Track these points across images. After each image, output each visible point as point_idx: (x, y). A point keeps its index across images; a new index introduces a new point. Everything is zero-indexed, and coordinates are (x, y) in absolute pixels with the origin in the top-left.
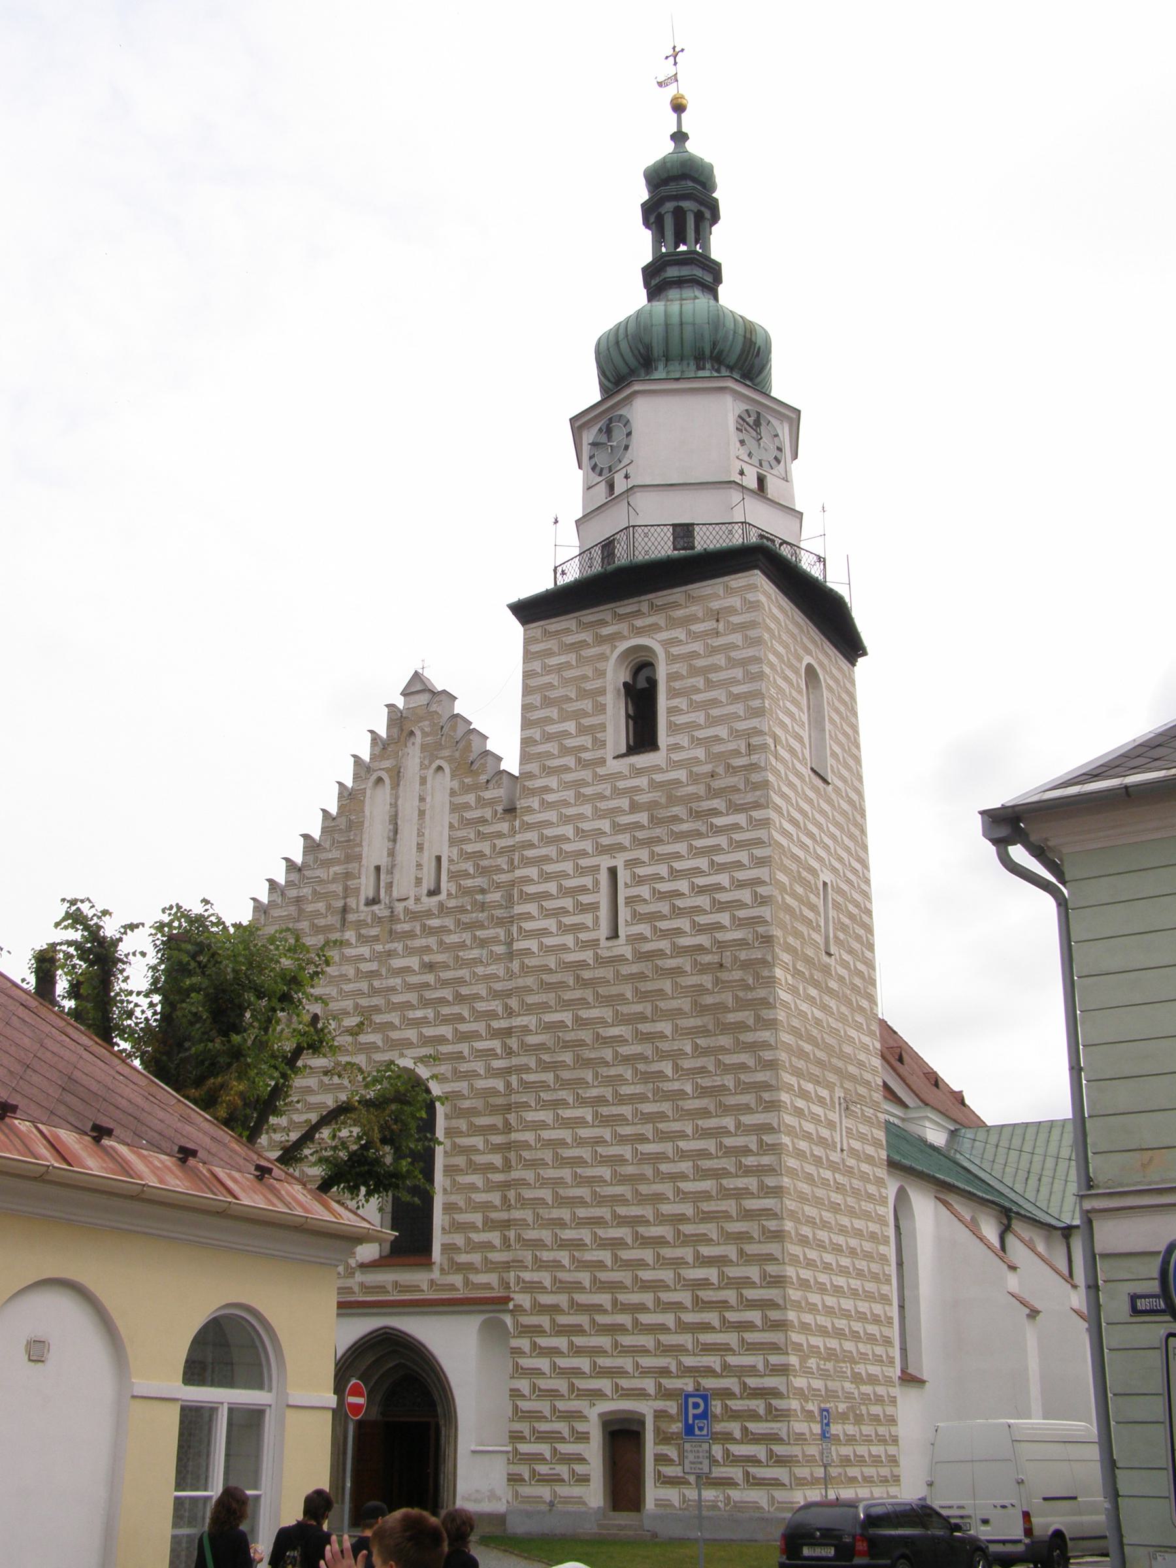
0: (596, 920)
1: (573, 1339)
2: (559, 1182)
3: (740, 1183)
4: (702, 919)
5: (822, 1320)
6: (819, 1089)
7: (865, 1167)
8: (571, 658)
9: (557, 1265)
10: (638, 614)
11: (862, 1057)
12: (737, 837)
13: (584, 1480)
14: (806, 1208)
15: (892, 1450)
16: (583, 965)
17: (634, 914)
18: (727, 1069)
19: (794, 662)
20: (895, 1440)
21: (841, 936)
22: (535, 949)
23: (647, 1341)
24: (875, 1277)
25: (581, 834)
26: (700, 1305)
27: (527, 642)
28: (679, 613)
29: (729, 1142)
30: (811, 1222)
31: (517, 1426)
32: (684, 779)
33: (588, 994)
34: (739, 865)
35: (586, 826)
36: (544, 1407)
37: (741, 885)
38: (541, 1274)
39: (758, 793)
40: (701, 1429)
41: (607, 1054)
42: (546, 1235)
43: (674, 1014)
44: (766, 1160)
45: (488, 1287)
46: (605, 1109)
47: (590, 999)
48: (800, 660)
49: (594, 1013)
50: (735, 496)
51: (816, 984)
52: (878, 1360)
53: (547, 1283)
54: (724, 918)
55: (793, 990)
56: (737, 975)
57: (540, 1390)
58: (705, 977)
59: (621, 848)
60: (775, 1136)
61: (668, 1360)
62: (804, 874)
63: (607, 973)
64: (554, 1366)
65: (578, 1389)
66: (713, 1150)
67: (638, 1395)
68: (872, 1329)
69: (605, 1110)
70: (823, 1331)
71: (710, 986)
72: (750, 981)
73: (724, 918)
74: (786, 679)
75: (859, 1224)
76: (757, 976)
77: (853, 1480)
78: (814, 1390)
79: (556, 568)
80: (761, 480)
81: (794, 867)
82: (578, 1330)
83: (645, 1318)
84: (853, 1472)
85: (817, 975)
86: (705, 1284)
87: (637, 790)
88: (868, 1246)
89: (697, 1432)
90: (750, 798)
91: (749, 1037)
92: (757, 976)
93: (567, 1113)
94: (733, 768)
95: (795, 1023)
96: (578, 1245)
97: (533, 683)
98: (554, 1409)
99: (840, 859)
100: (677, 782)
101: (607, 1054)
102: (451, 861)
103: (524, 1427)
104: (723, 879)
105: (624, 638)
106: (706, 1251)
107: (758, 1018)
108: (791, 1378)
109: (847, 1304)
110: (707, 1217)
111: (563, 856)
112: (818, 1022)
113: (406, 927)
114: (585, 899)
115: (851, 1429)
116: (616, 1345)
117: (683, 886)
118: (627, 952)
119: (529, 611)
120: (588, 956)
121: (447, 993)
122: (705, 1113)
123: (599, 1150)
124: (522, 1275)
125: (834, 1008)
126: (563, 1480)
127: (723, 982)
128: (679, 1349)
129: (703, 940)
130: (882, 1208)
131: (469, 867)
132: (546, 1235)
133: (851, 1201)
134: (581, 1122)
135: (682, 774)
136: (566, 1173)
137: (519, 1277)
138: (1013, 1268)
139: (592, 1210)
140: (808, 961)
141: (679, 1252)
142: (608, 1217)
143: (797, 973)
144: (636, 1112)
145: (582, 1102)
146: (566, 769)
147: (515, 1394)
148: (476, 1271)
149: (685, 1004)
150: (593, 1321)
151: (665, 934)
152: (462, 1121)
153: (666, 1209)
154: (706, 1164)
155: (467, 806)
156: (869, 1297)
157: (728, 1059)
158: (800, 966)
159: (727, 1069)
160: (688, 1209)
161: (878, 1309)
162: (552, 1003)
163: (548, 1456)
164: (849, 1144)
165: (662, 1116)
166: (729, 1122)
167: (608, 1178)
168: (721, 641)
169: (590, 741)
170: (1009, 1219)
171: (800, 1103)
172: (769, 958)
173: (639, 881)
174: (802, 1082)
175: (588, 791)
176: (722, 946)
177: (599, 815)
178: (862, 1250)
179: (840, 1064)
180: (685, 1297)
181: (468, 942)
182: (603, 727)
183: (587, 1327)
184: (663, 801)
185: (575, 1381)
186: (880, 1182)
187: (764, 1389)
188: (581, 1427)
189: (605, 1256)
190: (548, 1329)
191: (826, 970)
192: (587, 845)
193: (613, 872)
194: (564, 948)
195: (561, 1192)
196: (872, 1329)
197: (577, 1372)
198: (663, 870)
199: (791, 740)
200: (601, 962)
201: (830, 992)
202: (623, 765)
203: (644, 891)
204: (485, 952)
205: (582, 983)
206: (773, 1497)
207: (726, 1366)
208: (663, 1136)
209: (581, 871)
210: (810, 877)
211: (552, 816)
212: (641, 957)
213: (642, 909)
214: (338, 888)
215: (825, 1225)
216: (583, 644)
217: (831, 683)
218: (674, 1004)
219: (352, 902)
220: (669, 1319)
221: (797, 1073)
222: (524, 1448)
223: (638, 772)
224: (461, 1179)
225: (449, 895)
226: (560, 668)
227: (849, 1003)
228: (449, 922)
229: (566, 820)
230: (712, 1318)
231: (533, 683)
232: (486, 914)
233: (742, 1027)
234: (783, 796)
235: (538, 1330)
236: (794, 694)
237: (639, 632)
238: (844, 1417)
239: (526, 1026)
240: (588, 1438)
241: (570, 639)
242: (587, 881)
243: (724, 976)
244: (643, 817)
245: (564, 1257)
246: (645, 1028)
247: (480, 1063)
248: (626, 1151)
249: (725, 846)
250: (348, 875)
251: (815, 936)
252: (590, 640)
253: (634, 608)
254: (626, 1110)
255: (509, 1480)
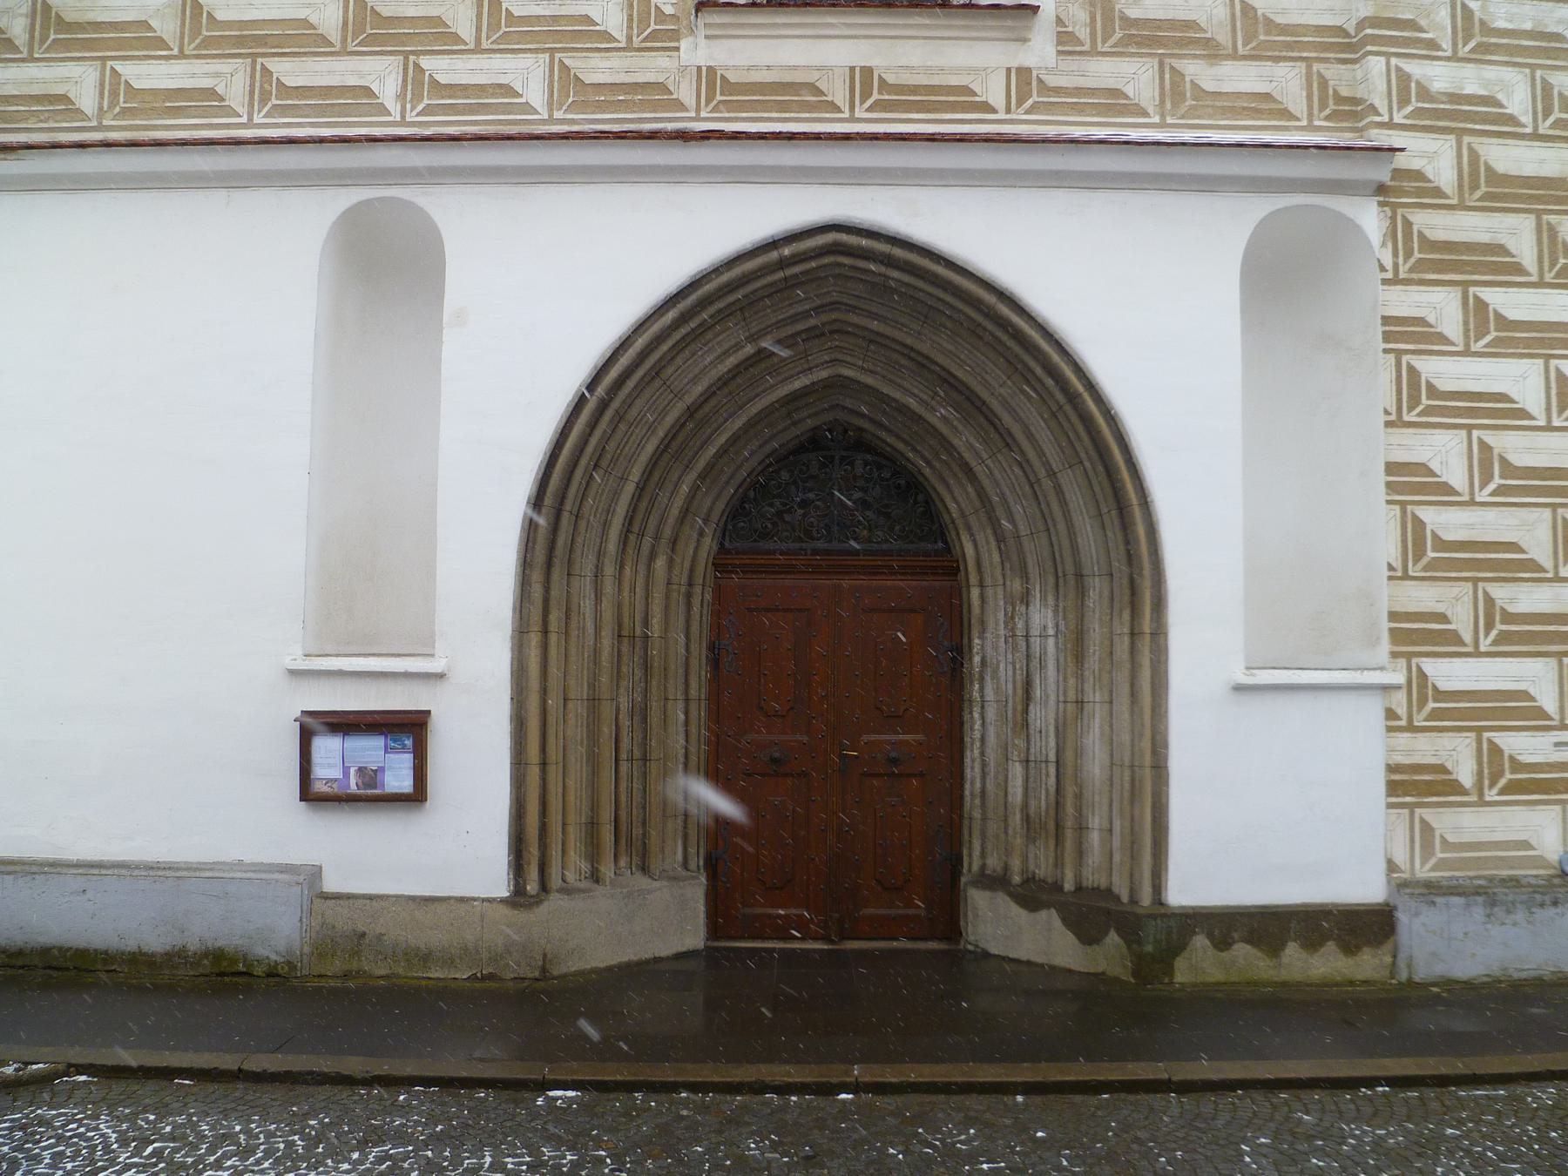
31: (1422, 597)
38: (1491, 72)
45: (1264, 105)
57: (1508, 469)
103: (1453, 601)
124: (1415, 69)
137: (1404, 78)
147: (1410, 483)
148: (1212, 52)
222: (1449, 673)
255: (1393, 788)
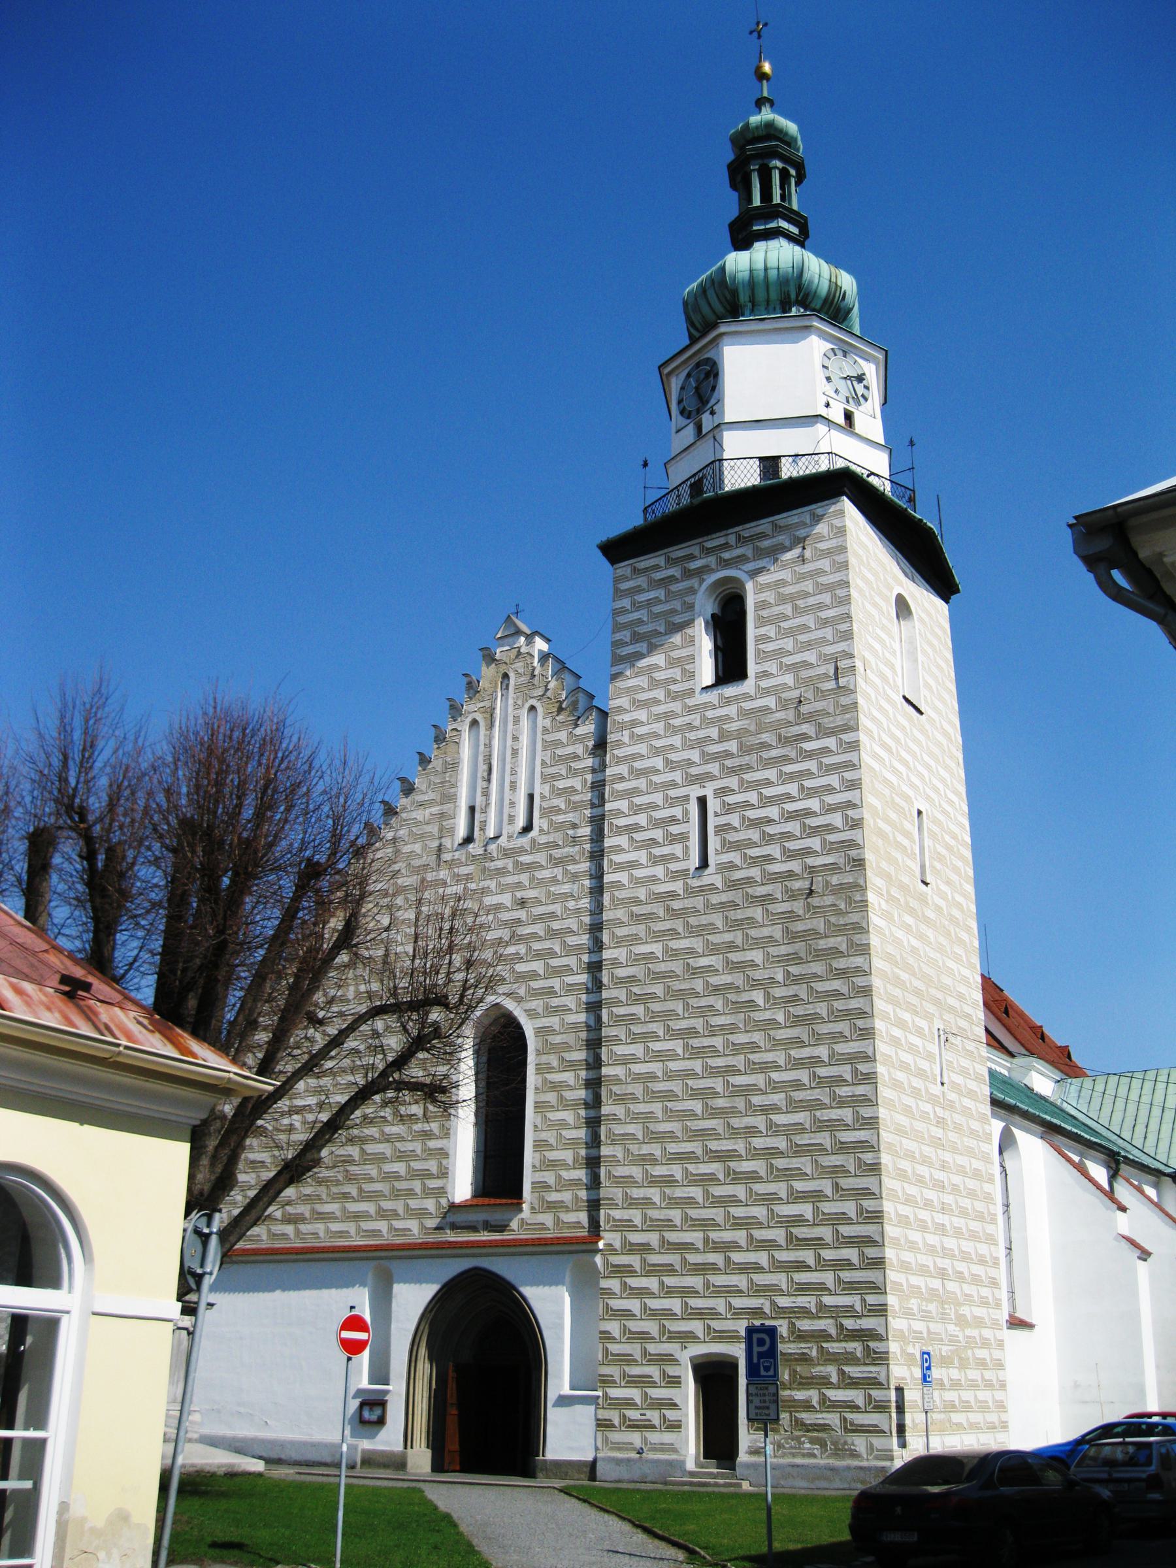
0: (686, 850)
1: (664, 1279)
2: (649, 1116)
3: (834, 1114)
4: (792, 845)
5: (923, 1259)
6: (917, 1019)
7: (967, 1102)
8: (660, 593)
9: (647, 1202)
10: (726, 546)
11: (962, 989)
12: (826, 761)
13: (676, 1426)
14: (905, 1141)
15: (999, 1395)
16: (673, 895)
17: (724, 842)
18: (819, 996)
19: (885, 591)
20: (1003, 1386)
21: (938, 865)
22: (625, 881)
23: (740, 1281)
24: (980, 1217)
25: (671, 765)
26: (795, 1242)
27: (617, 580)
28: (766, 543)
29: (822, 1071)
30: (910, 1156)
32: (773, 706)
33: (678, 925)
34: (829, 789)
35: (674, 757)
36: (635, 1349)
37: (831, 809)
39: (848, 716)
40: (767, 1369)
41: (698, 985)
42: (636, 1172)
43: (763, 943)
44: (860, 1090)
46: (696, 1041)
47: (680, 930)
48: (891, 589)
49: (684, 944)
50: (821, 428)
51: (912, 911)
52: (985, 1303)
53: (637, 1221)
54: (815, 843)
55: (887, 916)
56: (829, 900)
57: (630, 1332)
58: (795, 903)
59: (710, 777)
60: (870, 1065)
61: (761, 1300)
62: (897, 800)
63: (698, 902)
64: (645, 1307)
65: (670, 1332)
66: (806, 1080)
67: (731, 1337)
68: (977, 1269)
69: (695, 1043)
70: (924, 1271)
71: (801, 912)
72: (842, 906)
73: (815, 843)
74: (875, 605)
75: (961, 1160)
76: (849, 900)
77: (959, 1426)
78: (915, 1332)
79: (645, 510)
80: (849, 416)
81: (887, 792)
82: (669, 1270)
83: (737, 1257)
84: (957, 1418)
85: (913, 903)
86: (799, 1220)
87: (727, 719)
88: (971, 1184)
89: (763, 1373)
90: (839, 721)
91: (841, 963)
92: (849, 900)
93: (657, 1046)
94: (822, 691)
95: (890, 949)
96: (669, 1181)
97: (622, 619)
98: (645, 1352)
99: (936, 790)
100: (766, 710)
101: (698, 985)
102: (543, 797)
104: (814, 804)
105: (713, 571)
106: (799, 1186)
107: (851, 944)
108: (890, 1318)
109: (950, 1243)
110: (799, 1151)
111: (654, 788)
112: (914, 950)
113: (499, 864)
114: (675, 829)
115: (955, 1373)
116: (707, 1285)
117: (773, 812)
118: (718, 881)
119: (618, 550)
120: (678, 886)
121: (539, 929)
122: (798, 1043)
123: (690, 1082)
125: (931, 937)
126: (654, 1427)
127: (815, 907)
128: (775, 1289)
129: (795, 866)
130: (986, 1145)
131: (560, 803)
132: (636, 1172)
133: (952, 1136)
134: (671, 1055)
135: (771, 702)
136: (657, 1108)
137: (609, 1215)
138: (1123, 1209)
139: (684, 1145)
140: (903, 887)
141: (771, 1188)
142: (699, 1152)
143: (891, 899)
144: (727, 1043)
145: (672, 1034)
146: (656, 702)
148: (568, 1210)
149: (777, 932)
150: (684, 1261)
151: (754, 861)
152: (552, 1057)
153: (758, 1142)
154: (799, 1095)
155: (558, 743)
156: (974, 1236)
157: (821, 987)
158: (895, 892)
159: (819, 996)
160: (781, 1143)
161: (983, 1249)
162: (642, 935)
163: (638, 1401)
164: (949, 1077)
165: (754, 1047)
166: (822, 1052)
167: (699, 1112)
168: (808, 567)
169: (679, 673)
170: (1117, 1163)
171: (897, 1032)
172: (861, 882)
173: (729, 809)
174: (898, 1010)
175: (677, 722)
176: (812, 871)
177: (689, 745)
178: (966, 1188)
179: (939, 995)
180: (779, 1235)
181: (560, 877)
182: (692, 659)
183: (678, 1267)
184: (752, 728)
185: (666, 1323)
186: (982, 1119)
187: (862, 1330)
188: (671, 1371)
189: (696, 1192)
190: (638, 1270)
191: (923, 899)
192: (677, 776)
193: (702, 801)
194: (654, 879)
195: (652, 1127)
196: (977, 1269)
197: (668, 1314)
198: (752, 797)
199: (882, 666)
200: (691, 892)
201: (927, 921)
202: (713, 696)
203: (734, 820)
204: (576, 886)
205: (674, 914)
206: (872, 1445)
207: (821, 1306)
208: (754, 1068)
209: (671, 802)
210: (903, 804)
211: (642, 748)
212: (732, 885)
213: (732, 837)
214: (434, 829)
215: (925, 1161)
216: (672, 579)
217: (923, 615)
218: (766, 932)
219: (447, 842)
220: (762, 1258)
221: (894, 1002)
223: (728, 701)
224: (553, 1116)
225: (541, 831)
226: (650, 603)
227: (948, 934)
228: (541, 858)
229: (658, 751)
230: (808, 1256)
231: (622, 619)
232: (577, 848)
233: (835, 952)
234: (874, 719)
235: (628, 1270)
236: (885, 621)
237: (726, 564)
238: (946, 1362)
239: (616, 959)
240: (680, 1383)
241: (658, 575)
242: (677, 812)
243: (814, 901)
244: (733, 746)
245: (654, 1194)
246: (735, 957)
247: (570, 998)
248: (718, 1084)
249: (815, 770)
250: (442, 816)
251: (909, 863)
252: (678, 574)
253: (722, 541)
254: (718, 1042)
